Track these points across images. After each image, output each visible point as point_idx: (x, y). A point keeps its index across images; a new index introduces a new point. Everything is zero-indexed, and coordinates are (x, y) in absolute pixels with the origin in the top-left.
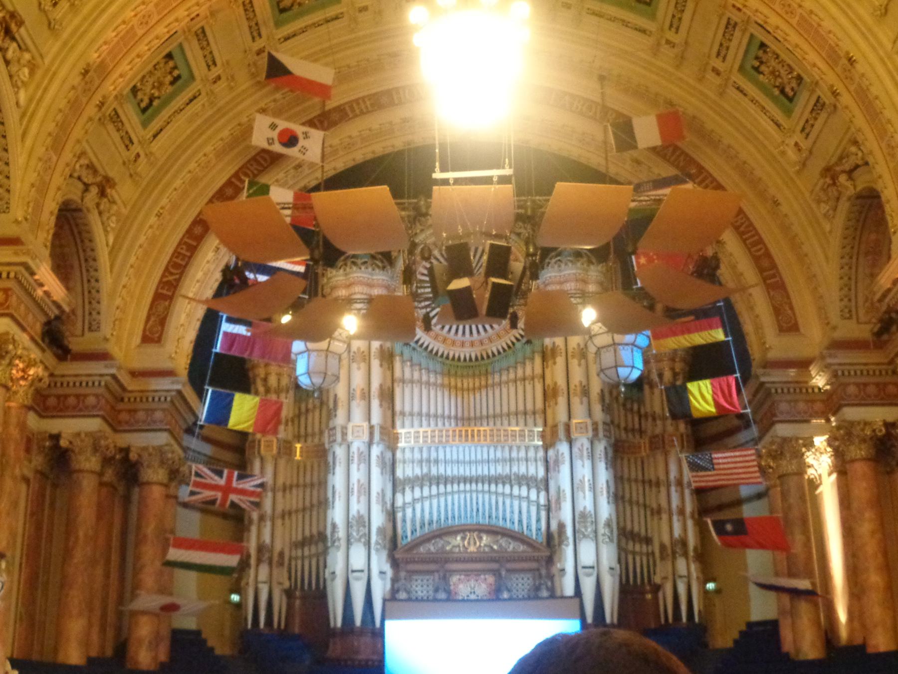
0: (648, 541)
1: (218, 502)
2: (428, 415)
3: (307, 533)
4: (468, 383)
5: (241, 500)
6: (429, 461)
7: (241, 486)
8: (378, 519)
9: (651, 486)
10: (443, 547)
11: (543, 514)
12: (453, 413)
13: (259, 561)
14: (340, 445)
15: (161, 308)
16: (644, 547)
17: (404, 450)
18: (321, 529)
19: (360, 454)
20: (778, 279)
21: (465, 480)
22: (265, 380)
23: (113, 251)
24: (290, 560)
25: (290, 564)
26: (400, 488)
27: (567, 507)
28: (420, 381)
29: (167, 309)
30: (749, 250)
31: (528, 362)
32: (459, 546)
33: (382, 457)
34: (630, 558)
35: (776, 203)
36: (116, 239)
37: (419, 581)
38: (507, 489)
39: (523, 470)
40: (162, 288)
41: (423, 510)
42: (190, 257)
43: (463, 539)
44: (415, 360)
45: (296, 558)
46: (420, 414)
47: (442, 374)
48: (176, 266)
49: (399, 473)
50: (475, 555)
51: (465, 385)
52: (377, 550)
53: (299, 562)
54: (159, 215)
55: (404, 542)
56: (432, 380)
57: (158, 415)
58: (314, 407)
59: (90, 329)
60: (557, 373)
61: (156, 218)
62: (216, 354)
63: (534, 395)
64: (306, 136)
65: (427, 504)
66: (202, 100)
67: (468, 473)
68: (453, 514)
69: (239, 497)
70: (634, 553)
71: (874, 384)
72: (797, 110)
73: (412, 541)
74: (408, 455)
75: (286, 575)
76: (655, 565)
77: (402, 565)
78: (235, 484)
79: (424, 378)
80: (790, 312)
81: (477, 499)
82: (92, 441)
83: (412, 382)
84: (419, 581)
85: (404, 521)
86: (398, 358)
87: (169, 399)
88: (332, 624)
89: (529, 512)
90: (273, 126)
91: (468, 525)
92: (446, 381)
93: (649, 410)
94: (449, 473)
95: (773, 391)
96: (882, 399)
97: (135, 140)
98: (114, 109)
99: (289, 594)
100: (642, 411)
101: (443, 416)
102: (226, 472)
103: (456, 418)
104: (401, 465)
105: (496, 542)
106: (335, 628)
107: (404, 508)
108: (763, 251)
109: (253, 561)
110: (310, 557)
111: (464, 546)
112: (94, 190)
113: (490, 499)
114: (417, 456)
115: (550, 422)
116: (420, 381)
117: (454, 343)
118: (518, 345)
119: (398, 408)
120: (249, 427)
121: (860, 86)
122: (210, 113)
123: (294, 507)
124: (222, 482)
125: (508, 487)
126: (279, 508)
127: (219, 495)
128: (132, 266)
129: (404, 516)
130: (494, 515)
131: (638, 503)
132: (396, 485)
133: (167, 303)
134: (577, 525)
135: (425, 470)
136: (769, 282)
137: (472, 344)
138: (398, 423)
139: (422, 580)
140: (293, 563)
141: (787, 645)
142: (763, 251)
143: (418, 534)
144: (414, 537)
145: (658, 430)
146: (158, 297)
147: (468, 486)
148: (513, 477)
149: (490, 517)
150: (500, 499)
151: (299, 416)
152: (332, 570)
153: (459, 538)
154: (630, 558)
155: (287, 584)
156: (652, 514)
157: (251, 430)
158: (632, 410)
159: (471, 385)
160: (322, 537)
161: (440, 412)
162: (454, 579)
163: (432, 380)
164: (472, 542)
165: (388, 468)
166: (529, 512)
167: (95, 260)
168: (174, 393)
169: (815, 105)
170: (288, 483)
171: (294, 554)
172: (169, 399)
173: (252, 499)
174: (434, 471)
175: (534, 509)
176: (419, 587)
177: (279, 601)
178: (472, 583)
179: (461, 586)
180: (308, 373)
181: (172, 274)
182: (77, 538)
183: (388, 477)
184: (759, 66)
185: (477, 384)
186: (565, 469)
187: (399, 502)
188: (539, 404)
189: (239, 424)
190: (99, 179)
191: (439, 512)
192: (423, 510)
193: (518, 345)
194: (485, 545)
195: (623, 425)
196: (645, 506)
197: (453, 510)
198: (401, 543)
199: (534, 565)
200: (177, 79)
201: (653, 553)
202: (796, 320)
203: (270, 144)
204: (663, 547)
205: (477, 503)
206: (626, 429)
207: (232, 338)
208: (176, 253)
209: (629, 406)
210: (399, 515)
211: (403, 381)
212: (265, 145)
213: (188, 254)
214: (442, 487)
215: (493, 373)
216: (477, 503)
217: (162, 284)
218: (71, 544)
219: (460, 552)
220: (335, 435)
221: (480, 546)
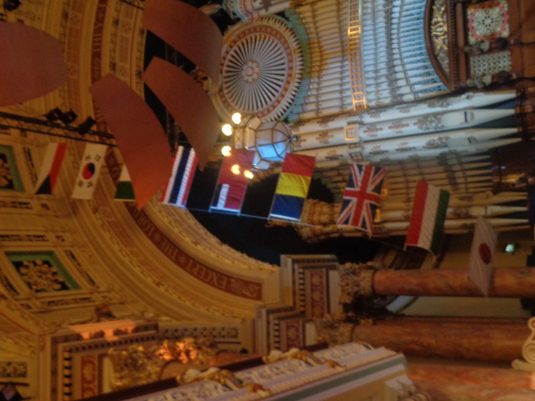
1: (373, 202)
2: (341, 85)
3: (444, 175)
4: (316, 57)
5: (373, 182)
6: (376, 78)
7: (360, 184)
8: (423, 109)
10: (445, 52)
12: (339, 64)
14: (363, 148)
17: (369, 101)
18: (435, 163)
19: (369, 130)
22: (325, 224)
23: (178, 317)
26: (399, 98)
28: (317, 96)
29: (237, 280)
32: (444, 40)
33: (372, 115)
36: (166, 314)
37: (475, 69)
38: (396, 10)
40: (222, 285)
41: (416, 76)
42: (201, 264)
44: (302, 102)
45: (467, 189)
46: (341, 92)
47: (311, 78)
48: (206, 276)
49: (387, 101)
50: (450, 25)
52: (448, 105)
53: (471, 185)
54: (158, 284)
55: (444, 88)
56: (315, 86)
57: (316, 280)
59: (235, 337)
61: (161, 287)
62: (242, 212)
64: (88, 158)
66: (76, 251)
68: (417, 49)
69: (369, 184)
74: (372, 96)
75: (481, 195)
77: (462, 84)
78: (357, 189)
79: (314, 92)
81: (404, 32)
82: (325, 330)
83: (317, 103)
84: (475, 69)
85: (425, 91)
86: (301, 116)
87: (301, 270)
90: (81, 184)
91: (425, 37)
92: (316, 74)
97: (89, 296)
99: (498, 188)
101: (341, 73)
102: (346, 198)
103: (342, 62)
104: (381, 101)
105: (439, 9)
107: (415, 93)
110: (466, 177)
113: (404, 22)
114: (372, 88)
116: (317, 96)
117: (290, 75)
118: (290, 25)
119: (336, 110)
120: (305, 179)
122: (92, 248)
124: (355, 200)
127: (366, 202)
128: (194, 305)
129: (421, 91)
130: (416, 16)
135: (383, 79)
137: (291, 61)
138: (349, 108)
139: (475, 67)
140: (471, 190)
143: (435, 76)
144: (439, 80)
146: (228, 289)
147: (395, 41)
149: (419, 19)
152: (467, 143)
155: (490, 193)
157: (309, 178)
160: (442, 159)
161: (338, 76)
163: (315, 86)
167: (176, 330)
171: (463, 191)
172: (301, 270)
173: (372, 173)
174: (384, 72)
176: (480, 68)
178: (475, 24)
179: (478, 33)
180: (273, 144)
181: (212, 279)
187: (410, 97)
189: (303, 189)
191: (416, 62)
192: (416, 76)
194: (442, 17)
197: (414, 50)
198: (445, 89)
203: (92, 185)
205: (408, 31)
207: (230, 201)
208: (198, 276)
210: (421, 95)
211: (318, 110)
212: (92, 189)
213: (198, 265)
215: (309, 39)
216: (408, 31)
217: (219, 286)
218: (418, 348)
219: (448, 38)
220: (355, 153)
221: (443, 22)
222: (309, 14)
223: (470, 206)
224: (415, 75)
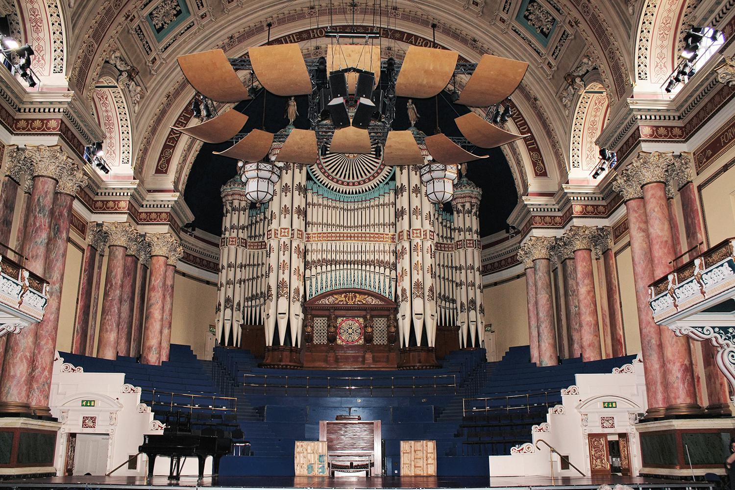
0: (454, 301)
9: (456, 270)
11: (393, 284)
13: (226, 307)
15: (167, 154)
16: (451, 304)
20: (535, 145)
21: (347, 262)
24: (244, 308)
25: (244, 310)
27: (407, 279)
30: (519, 128)
31: (386, 195)
34: (443, 310)
35: (536, 99)
39: (382, 258)
43: (345, 297)
51: (349, 208)
53: (249, 309)
58: (261, 220)
60: (403, 202)
63: (388, 215)
65: (324, 276)
67: (349, 259)
70: (445, 308)
71: (591, 205)
72: (551, 41)
73: (315, 297)
75: (241, 316)
76: (457, 315)
80: (541, 164)
88: (267, 345)
89: (384, 282)
93: (456, 226)
94: (338, 258)
95: (532, 210)
96: (596, 214)
98: (139, 25)
100: (452, 227)
106: (269, 346)
108: (526, 129)
109: (222, 308)
111: (346, 300)
112: (125, 75)
115: (398, 230)
118: (381, 185)
119: (309, 219)
121: (593, 15)
123: (247, 278)
125: (372, 267)
126: (238, 278)
131: (448, 279)
132: (307, 265)
133: (171, 151)
134: (413, 289)
136: (529, 147)
140: (246, 309)
141: (535, 358)
142: (526, 129)
145: (462, 237)
148: (376, 261)
150: (368, 274)
151: (251, 225)
153: (343, 296)
154: (443, 310)
155: (242, 322)
156: (457, 286)
158: (446, 226)
159: (352, 208)
162: (340, 320)
164: (350, 299)
165: (302, 255)
166: (384, 282)
168: (173, 203)
169: (562, 37)
170: (244, 263)
175: (387, 280)
177: (237, 331)
182: (112, 285)
183: (301, 260)
184: (528, 15)
185: (356, 207)
186: (407, 257)
188: (392, 220)
190: (129, 68)
193: (381, 185)
195: (441, 234)
196: (452, 281)
199: (386, 313)
200: (179, 12)
201: (456, 308)
202: (545, 169)
204: (462, 304)
206: (442, 237)
209: (444, 224)
214: (333, 266)
222: (387, 201)
223: (232, 310)
224: (323, 280)
